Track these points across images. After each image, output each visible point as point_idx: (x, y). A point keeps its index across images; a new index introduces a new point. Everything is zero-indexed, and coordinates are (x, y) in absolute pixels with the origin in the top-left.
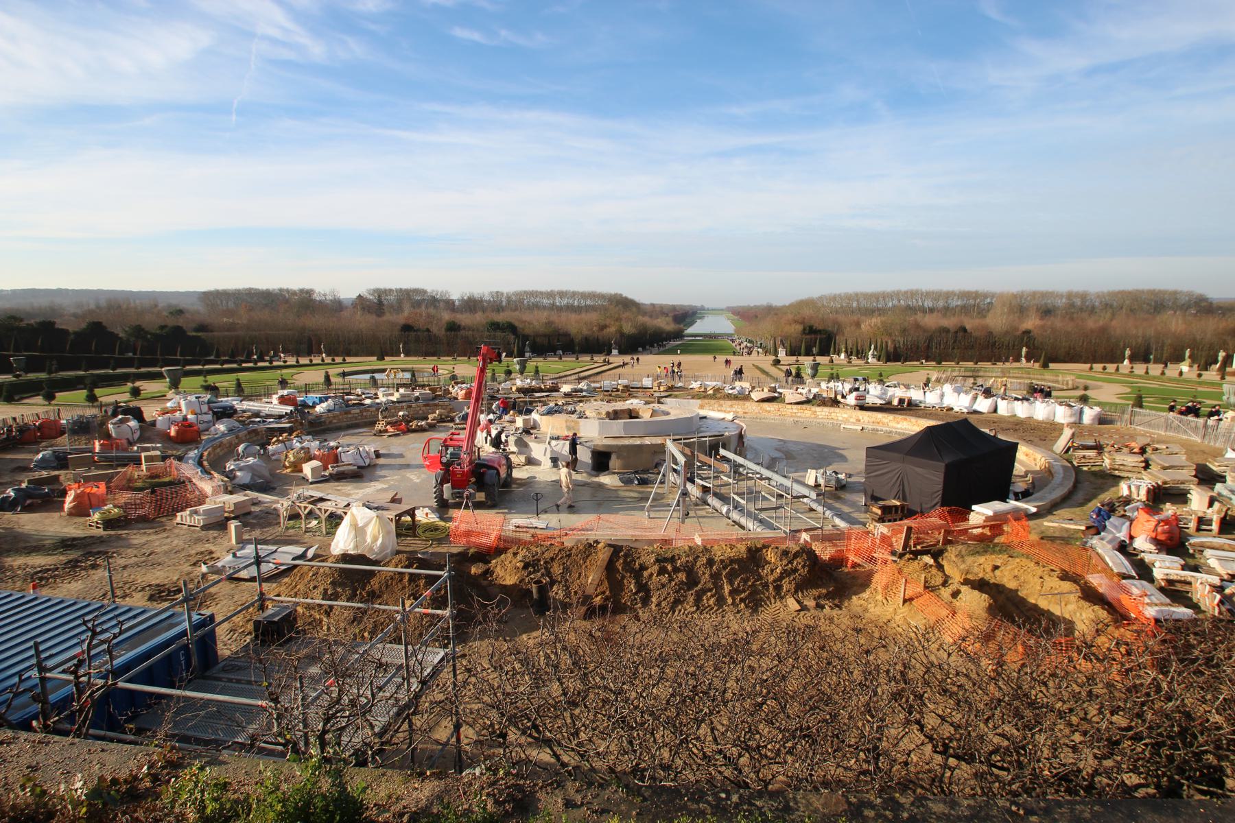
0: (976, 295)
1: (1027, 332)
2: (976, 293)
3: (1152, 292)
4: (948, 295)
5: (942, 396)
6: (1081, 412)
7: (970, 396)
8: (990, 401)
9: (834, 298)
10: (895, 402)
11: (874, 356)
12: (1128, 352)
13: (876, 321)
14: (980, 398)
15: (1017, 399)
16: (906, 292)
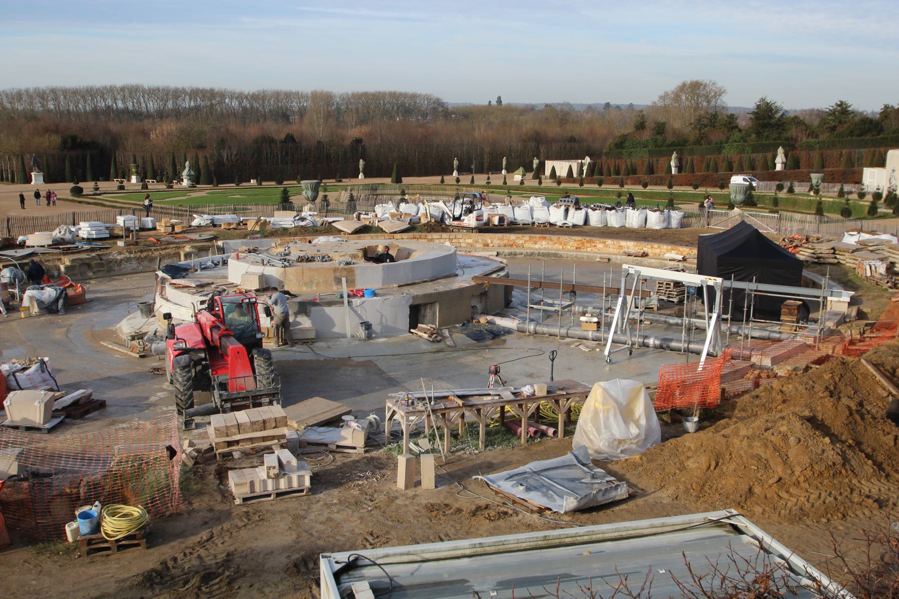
0: (211, 94)
1: (358, 141)
2: (212, 90)
3: (393, 95)
4: (177, 94)
5: (532, 209)
6: (669, 217)
7: (563, 208)
8: (583, 212)
9: (19, 96)
10: (496, 221)
12: (456, 162)
13: (170, 127)
14: (572, 211)
15: (607, 208)
16: (123, 89)
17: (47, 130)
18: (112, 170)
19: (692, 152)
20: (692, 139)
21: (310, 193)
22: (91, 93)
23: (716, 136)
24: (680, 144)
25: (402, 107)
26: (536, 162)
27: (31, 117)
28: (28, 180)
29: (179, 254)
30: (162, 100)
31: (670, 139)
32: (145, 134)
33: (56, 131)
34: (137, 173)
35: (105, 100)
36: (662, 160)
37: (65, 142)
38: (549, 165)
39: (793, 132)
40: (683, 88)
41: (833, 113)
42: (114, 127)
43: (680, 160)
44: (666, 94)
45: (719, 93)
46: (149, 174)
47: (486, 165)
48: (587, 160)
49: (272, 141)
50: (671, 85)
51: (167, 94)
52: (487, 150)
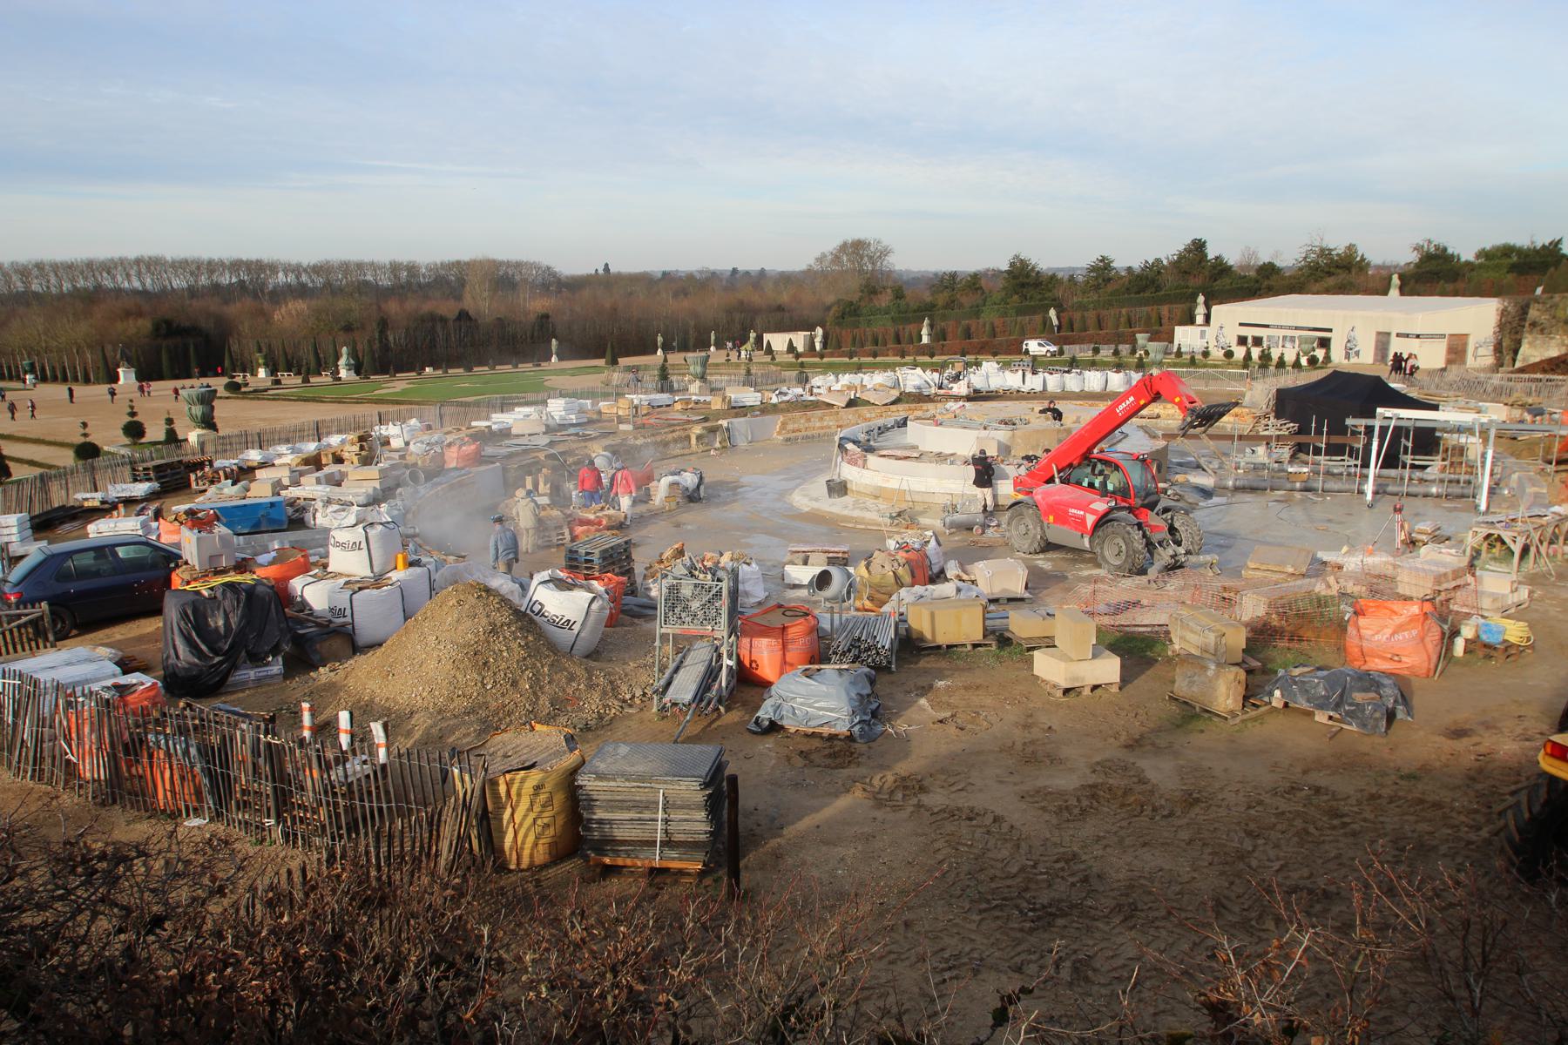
1: (545, 317)
11: (349, 367)
12: (660, 339)
17: (127, 314)
18: (227, 363)
19: (944, 317)
20: (940, 302)
21: (699, 369)
22: (90, 267)
23: (967, 300)
24: (927, 310)
25: (503, 278)
26: (753, 335)
27: (93, 297)
28: (115, 379)
29: (688, 438)
30: (192, 274)
31: (914, 305)
32: (265, 316)
33: (140, 314)
34: (266, 365)
35: (114, 278)
36: (910, 328)
37: (157, 328)
38: (767, 337)
39: (1059, 293)
40: (844, 247)
41: (1093, 269)
42: (213, 305)
43: (931, 326)
44: (824, 256)
45: (885, 252)
46: (282, 364)
47: (691, 342)
48: (819, 331)
49: (443, 320)
50: (831, 245)
51: (198, 268)
52: (692, 323)
